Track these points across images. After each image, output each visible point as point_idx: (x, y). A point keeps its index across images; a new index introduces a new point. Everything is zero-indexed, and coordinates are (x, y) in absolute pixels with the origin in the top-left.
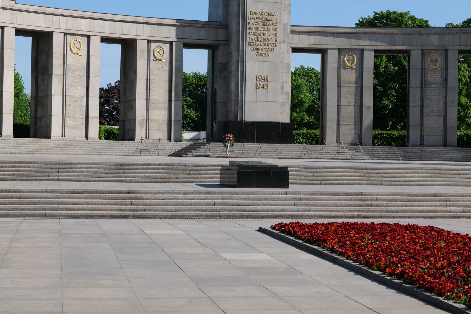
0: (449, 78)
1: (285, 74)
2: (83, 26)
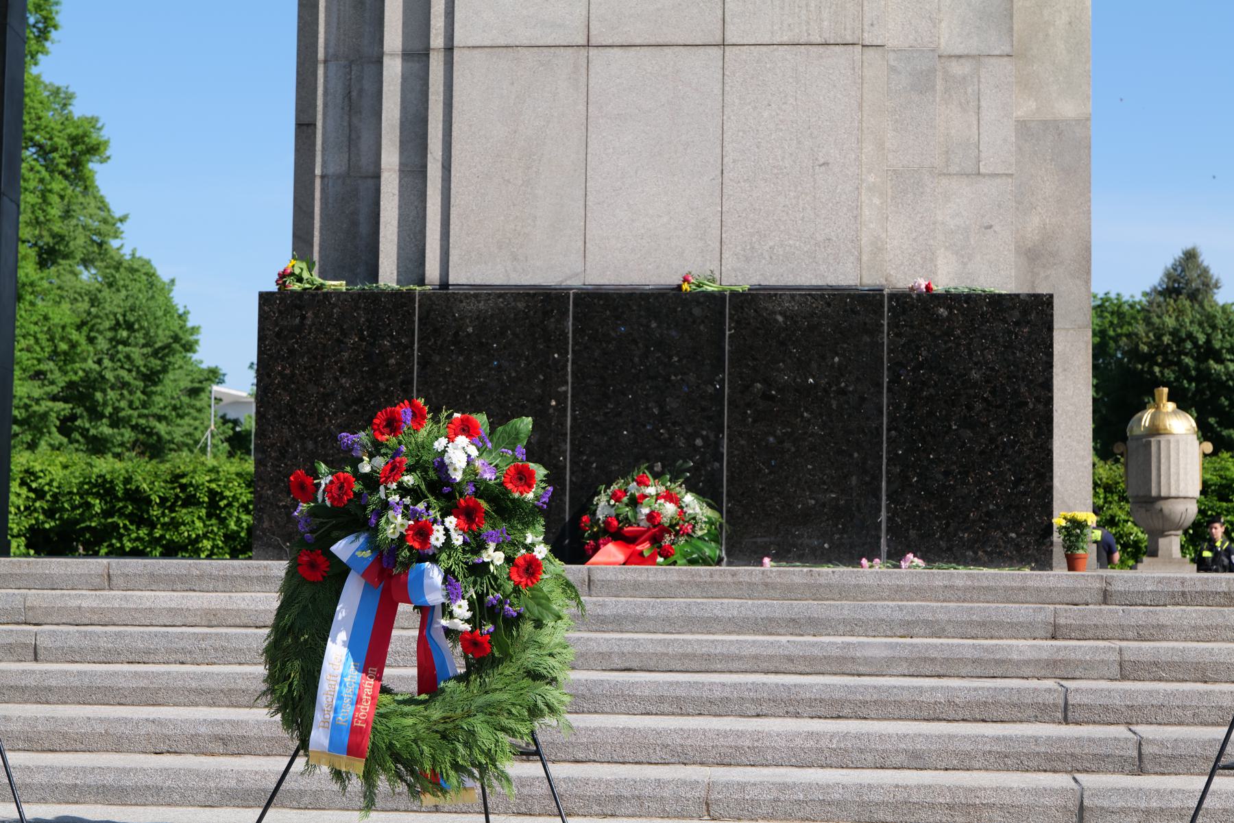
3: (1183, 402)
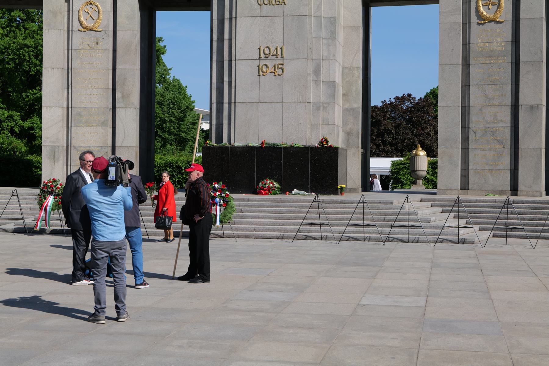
1: (323, 42)
3: (423, 148)
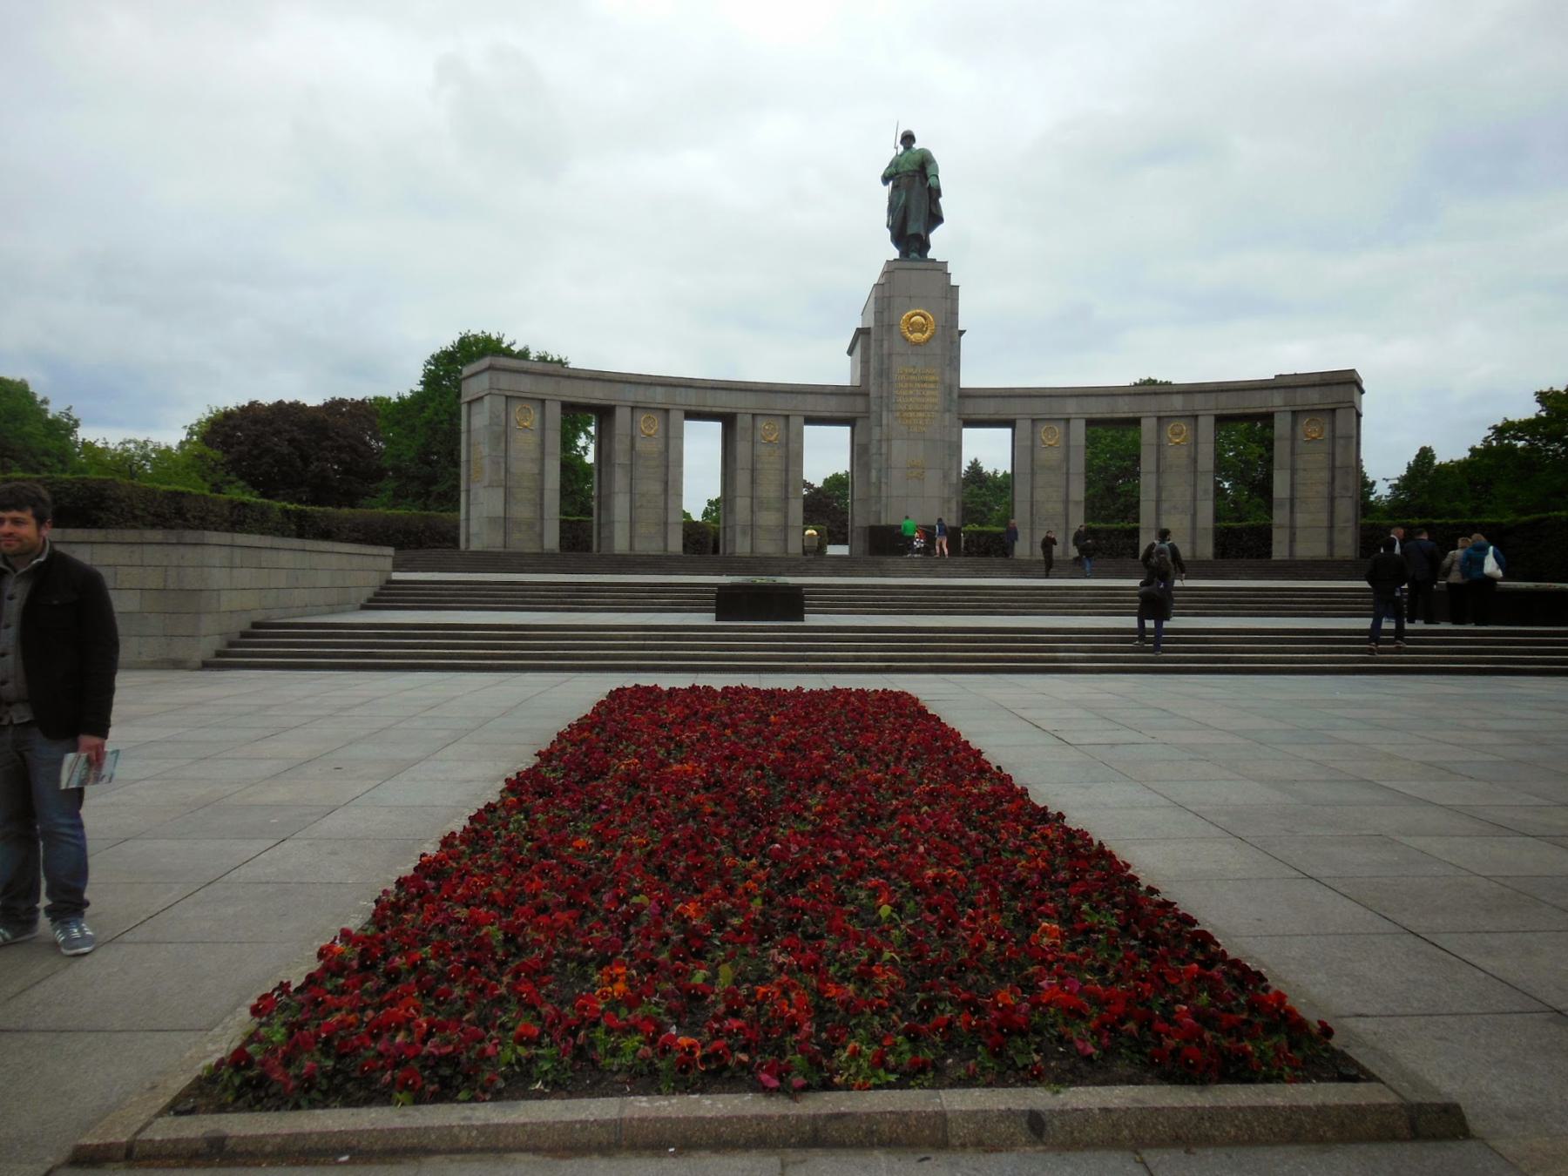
0: (1200, 457)
2: (659, 396)
